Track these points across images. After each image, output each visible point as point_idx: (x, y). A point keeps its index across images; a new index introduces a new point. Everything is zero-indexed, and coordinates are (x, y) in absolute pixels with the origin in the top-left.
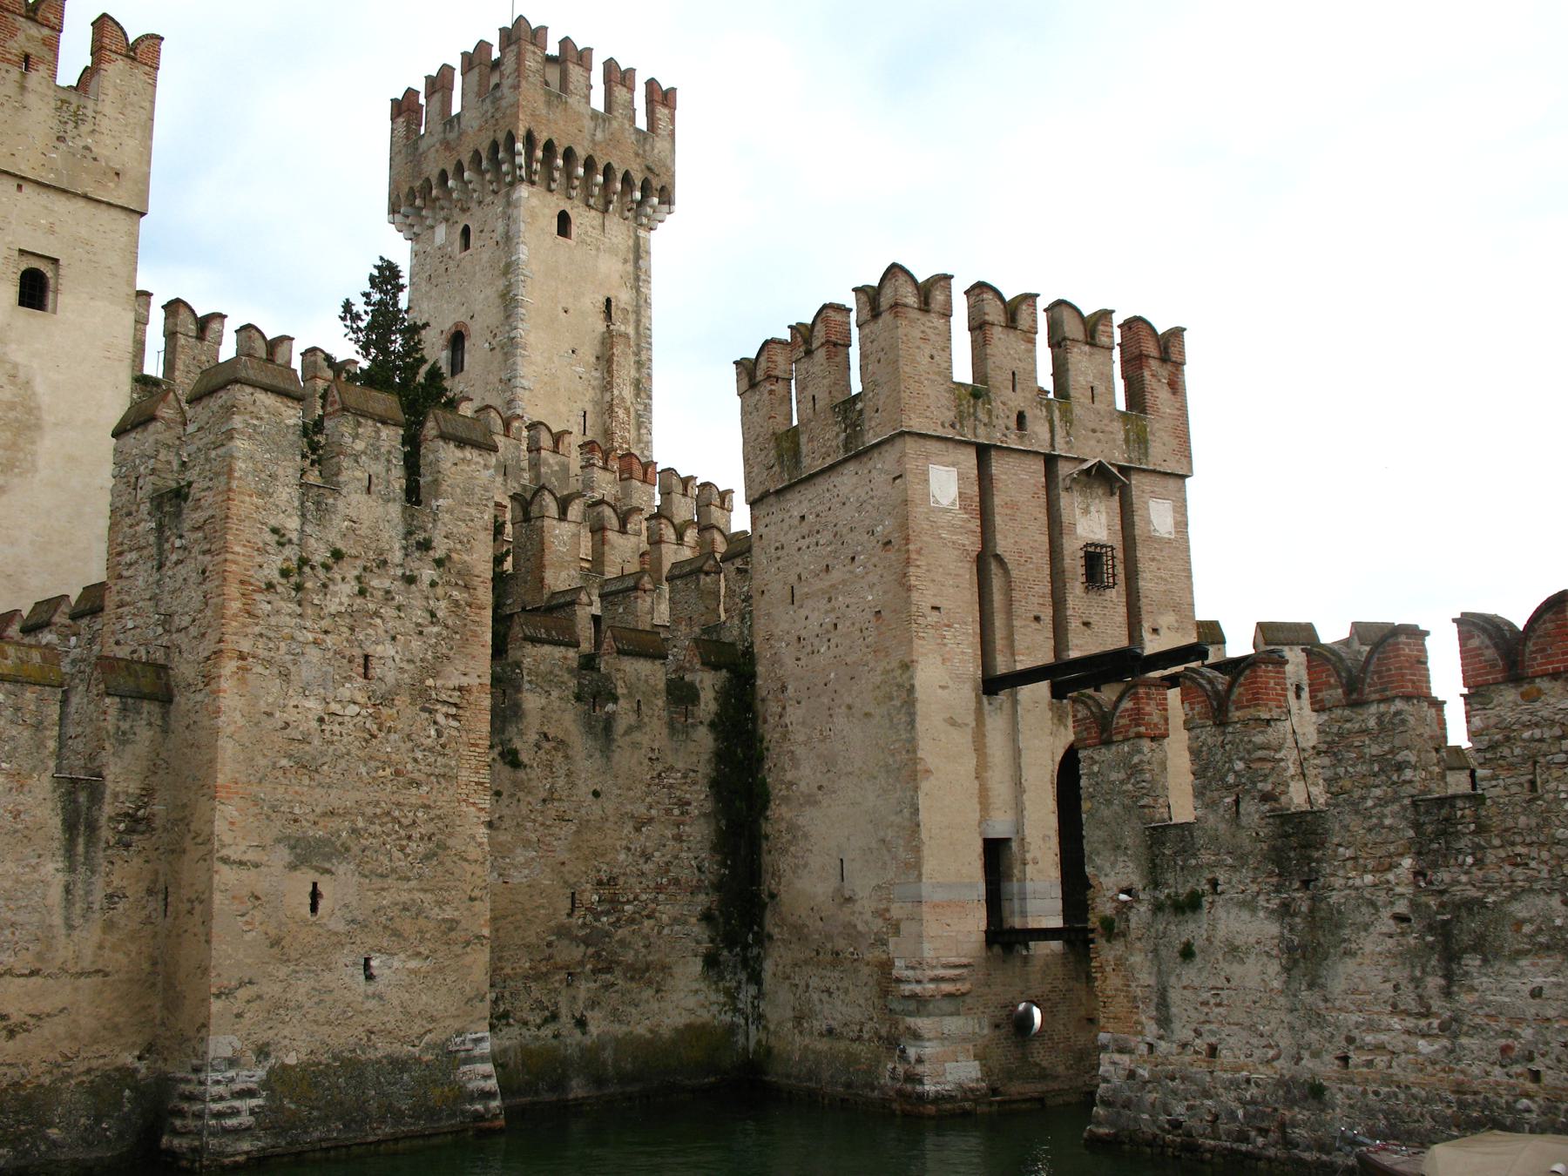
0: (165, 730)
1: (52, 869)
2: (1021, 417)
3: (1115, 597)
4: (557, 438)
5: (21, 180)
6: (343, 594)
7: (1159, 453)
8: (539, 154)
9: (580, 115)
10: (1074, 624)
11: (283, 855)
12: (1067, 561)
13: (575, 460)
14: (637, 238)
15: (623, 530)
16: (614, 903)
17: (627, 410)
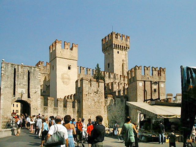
0: (80, 105)
1: (72, 114)
2: (148, 78)
3: (157, 93)
4: (117, 75)
5: (67, 59)
6: (92, 95)
7: (162, 80)
8: (115, 46)
9: (119, 41)
10: (153, 95)
11: (88, 114)
12: (152, 90)
13: (119, 76)
14: (126, 53)
15: (121, 85)
16: (116, 118)
17: (125, 71)
